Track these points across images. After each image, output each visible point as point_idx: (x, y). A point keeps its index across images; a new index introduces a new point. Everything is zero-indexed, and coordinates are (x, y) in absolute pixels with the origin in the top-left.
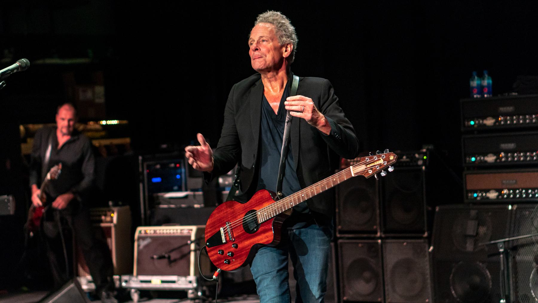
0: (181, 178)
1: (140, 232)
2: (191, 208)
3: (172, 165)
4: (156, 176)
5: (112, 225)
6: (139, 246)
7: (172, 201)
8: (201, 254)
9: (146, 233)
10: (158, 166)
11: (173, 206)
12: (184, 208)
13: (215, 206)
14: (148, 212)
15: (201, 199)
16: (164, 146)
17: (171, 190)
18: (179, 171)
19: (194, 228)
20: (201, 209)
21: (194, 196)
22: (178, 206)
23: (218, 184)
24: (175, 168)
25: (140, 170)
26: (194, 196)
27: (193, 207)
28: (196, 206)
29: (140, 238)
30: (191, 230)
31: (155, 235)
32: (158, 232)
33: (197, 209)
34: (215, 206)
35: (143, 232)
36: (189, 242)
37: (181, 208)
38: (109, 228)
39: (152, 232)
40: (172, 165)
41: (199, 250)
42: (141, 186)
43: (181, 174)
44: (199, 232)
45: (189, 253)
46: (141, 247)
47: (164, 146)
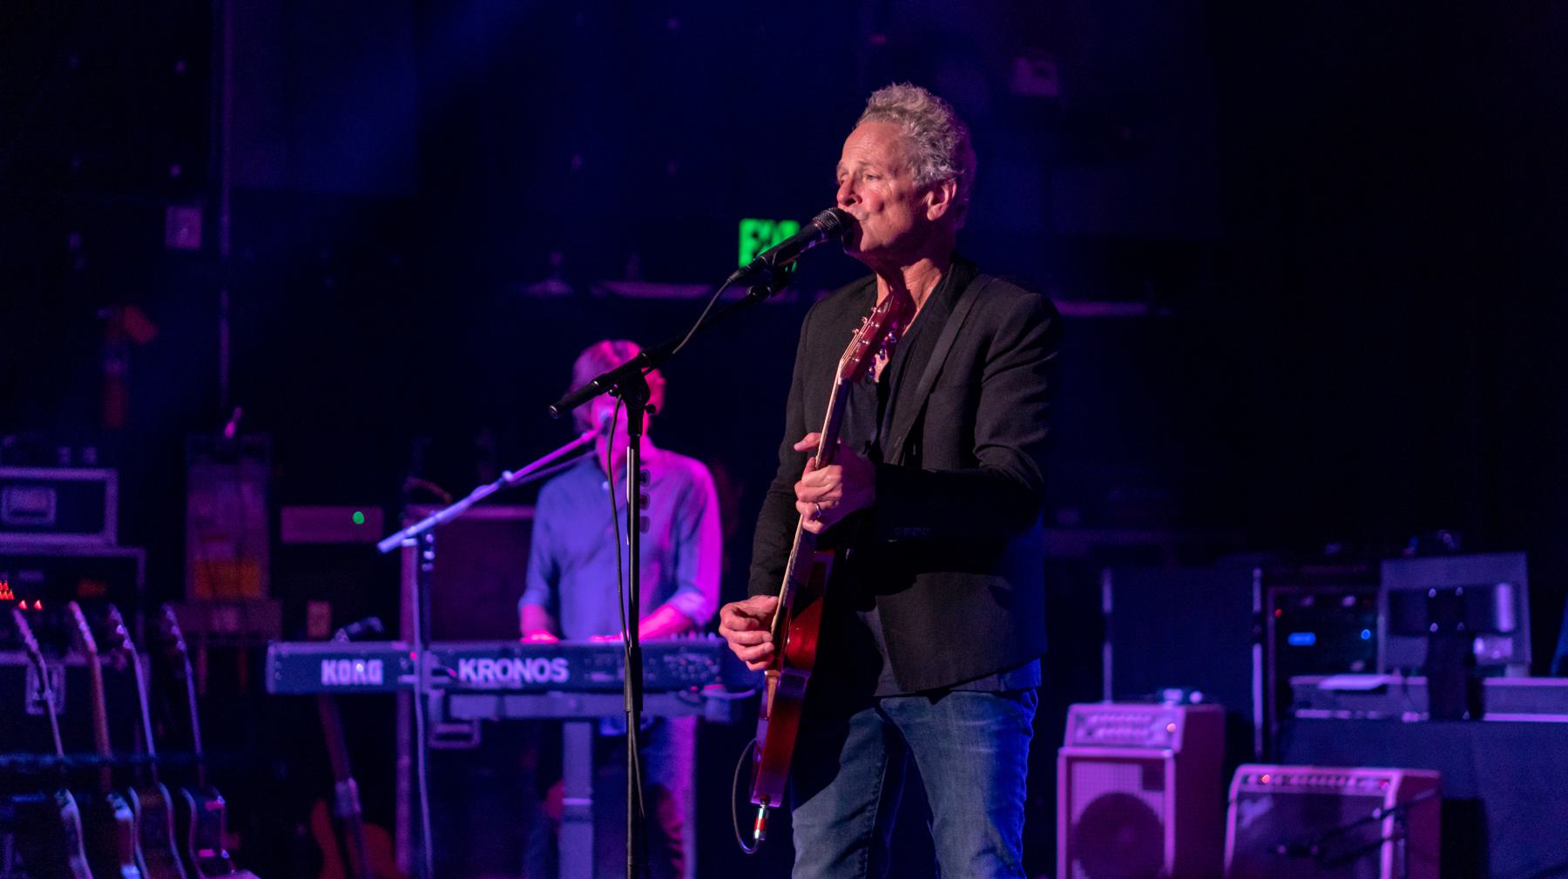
0: (1374, 640)
1: (1245, 780)
2: (1392, 721)
3: (1349, 601)
4: (1302, 629)
5: (1167, 754)
6: (1239, 818)
7: (1342, 698)
8: (1407, 847)
9: (1260, 783)
10: (1308, 601)
11: (1343, 714)
12: (1374, 721)
13: (1459, 718)
14: (1274, 728)
15: (1422, 697)
16: (1332, 548)
17: (1345, 669)
18: (1369, 618)
19: (1395, 776)
20: (1421, 723)
21: (1405, 688)
22: (1359, 714)
23: (1470, 657)
24: (1357, 609)
25: (1257, 606)
26: (1405, 688)
27: (1400, 722)
28: (1408, 717)
29: (1242, 797)
30: (1388, 780)
31: (1286, 790)
32: (1294, 781)
33: (1411, 724)
34: (1459, 718)
35: (1252, 780)
36: (1377, 813)
37: (1366, 720)
38: (1161, 762)
39: (1279, 780)
40: (1349, 601)
41: (1406, 837)
42: (1257, 652)
43: (1373, 627)
44: (1406, 786)
45: (1380, 842)
46: (1246, 822)
47: (1332, 548)
